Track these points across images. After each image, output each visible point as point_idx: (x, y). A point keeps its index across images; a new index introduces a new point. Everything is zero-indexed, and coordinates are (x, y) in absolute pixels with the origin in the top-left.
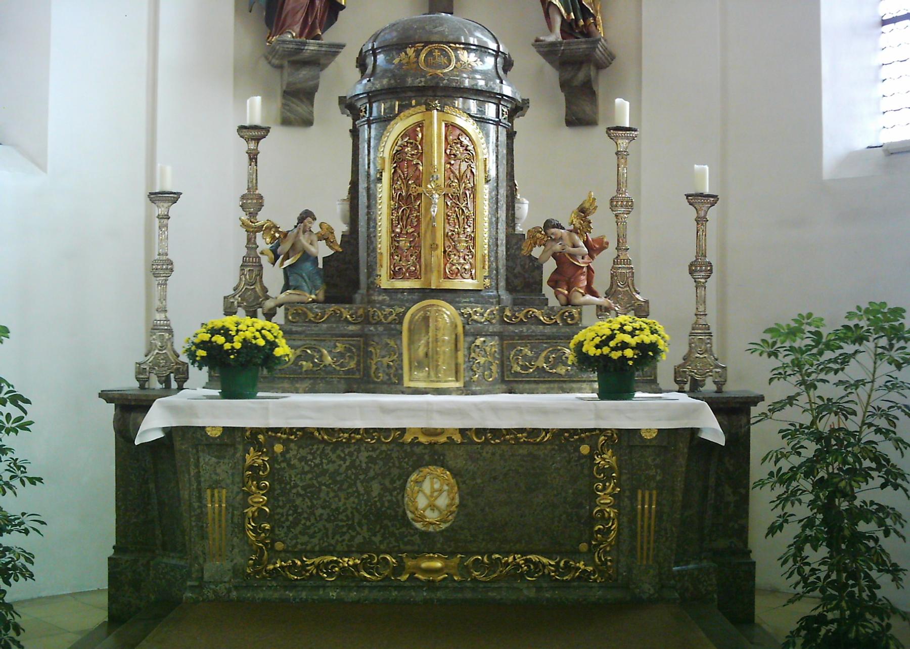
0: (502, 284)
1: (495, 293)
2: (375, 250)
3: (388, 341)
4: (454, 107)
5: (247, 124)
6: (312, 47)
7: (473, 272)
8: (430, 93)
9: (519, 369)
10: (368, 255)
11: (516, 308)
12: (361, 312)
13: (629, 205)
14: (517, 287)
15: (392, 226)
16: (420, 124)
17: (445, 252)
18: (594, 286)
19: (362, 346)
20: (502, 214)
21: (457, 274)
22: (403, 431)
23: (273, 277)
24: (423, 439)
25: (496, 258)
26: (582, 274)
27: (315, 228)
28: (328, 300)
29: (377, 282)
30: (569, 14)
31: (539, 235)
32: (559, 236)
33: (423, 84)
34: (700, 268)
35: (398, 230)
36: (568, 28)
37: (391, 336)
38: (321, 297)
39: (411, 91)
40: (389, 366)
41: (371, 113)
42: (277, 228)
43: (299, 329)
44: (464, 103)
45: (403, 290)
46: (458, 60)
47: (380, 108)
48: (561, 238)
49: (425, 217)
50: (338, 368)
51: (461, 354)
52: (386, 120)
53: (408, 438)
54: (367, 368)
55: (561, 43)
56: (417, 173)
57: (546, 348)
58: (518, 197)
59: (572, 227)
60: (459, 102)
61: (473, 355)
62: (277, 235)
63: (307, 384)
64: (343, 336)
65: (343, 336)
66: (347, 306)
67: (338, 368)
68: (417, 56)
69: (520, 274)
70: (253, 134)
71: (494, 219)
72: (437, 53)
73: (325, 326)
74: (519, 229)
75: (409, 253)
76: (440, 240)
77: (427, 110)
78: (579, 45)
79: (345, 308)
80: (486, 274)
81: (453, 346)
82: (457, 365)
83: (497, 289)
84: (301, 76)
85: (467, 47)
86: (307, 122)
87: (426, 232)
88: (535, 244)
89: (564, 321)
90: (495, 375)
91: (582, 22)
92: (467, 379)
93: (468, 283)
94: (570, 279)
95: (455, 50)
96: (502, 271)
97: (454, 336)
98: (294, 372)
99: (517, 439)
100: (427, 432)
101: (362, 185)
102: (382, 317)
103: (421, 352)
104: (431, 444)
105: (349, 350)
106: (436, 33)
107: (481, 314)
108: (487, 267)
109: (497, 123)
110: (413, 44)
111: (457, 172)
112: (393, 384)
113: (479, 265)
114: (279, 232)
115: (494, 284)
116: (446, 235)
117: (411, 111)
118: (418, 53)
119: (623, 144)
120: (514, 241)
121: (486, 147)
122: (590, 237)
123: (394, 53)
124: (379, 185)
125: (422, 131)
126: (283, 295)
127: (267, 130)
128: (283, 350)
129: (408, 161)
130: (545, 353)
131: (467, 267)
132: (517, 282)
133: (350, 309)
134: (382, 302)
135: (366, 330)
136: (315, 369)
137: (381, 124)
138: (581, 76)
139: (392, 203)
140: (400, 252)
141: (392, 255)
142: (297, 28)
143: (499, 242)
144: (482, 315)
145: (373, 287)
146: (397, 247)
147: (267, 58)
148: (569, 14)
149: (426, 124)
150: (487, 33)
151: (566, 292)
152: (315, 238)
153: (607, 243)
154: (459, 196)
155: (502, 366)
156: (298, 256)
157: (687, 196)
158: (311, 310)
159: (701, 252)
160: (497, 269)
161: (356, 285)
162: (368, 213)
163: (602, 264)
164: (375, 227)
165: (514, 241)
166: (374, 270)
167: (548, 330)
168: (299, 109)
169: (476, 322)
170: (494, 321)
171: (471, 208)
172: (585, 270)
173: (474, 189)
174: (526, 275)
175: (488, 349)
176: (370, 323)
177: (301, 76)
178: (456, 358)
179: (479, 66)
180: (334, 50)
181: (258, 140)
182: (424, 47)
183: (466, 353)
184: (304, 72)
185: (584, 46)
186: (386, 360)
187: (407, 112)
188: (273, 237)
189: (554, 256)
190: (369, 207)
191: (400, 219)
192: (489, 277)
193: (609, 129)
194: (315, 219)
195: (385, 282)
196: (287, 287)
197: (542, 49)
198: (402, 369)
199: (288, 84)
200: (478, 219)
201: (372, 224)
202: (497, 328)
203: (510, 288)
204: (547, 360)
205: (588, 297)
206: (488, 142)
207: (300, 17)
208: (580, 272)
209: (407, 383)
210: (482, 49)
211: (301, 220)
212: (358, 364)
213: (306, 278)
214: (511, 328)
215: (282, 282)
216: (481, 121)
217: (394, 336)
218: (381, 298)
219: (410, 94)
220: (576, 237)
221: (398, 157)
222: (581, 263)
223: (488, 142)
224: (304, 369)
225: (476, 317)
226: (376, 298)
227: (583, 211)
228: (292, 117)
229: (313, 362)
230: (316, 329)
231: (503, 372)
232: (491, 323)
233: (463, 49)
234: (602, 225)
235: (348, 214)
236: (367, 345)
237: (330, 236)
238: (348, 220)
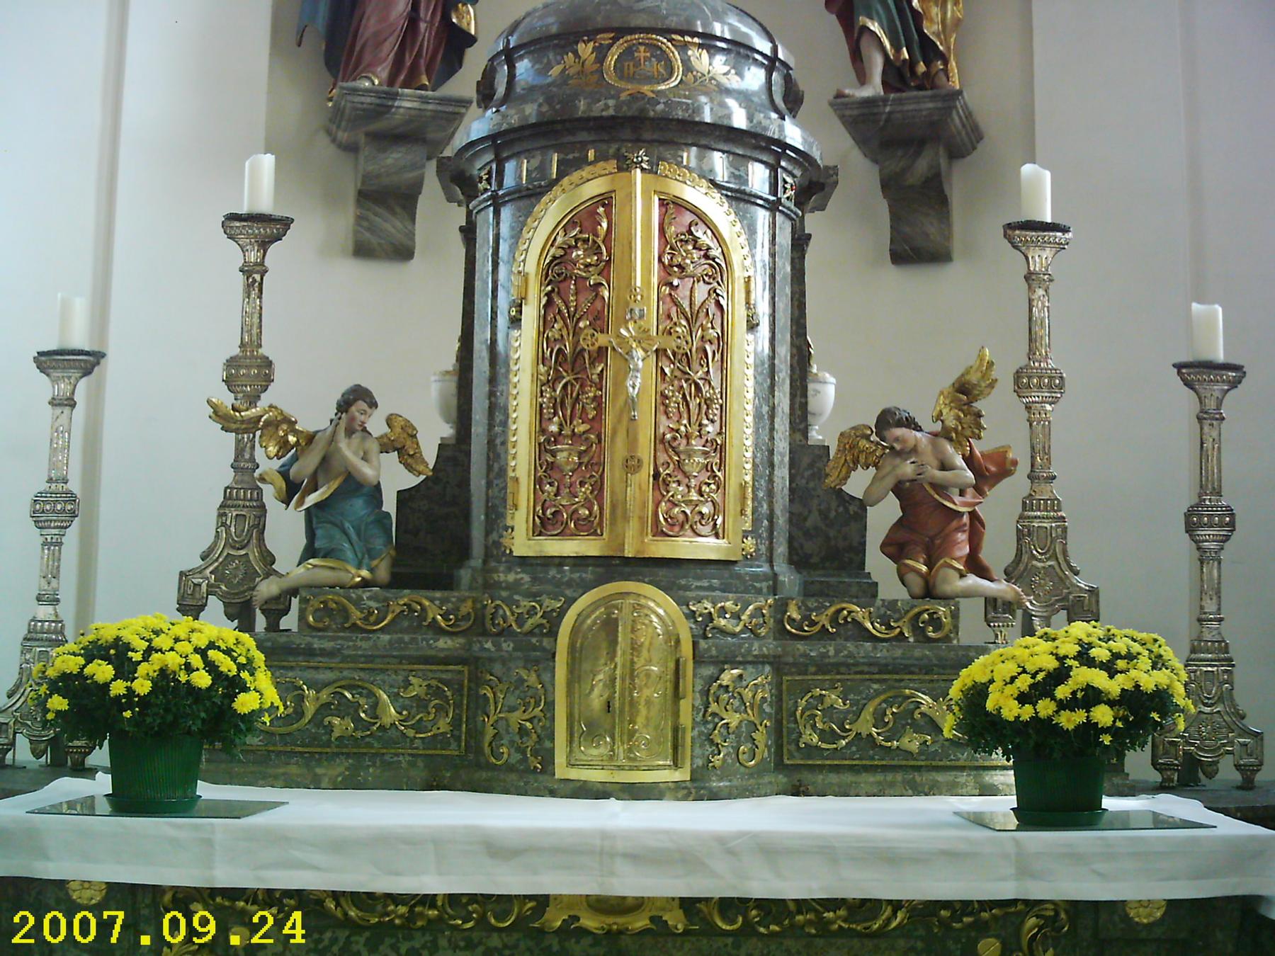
0: (781, 549)
1: (765, 568)
2: (503, 472)
3: (524, 674)
4: (679, 164)
5: (244, 210)
6: (407, 102)
7: (719, 521)
8: (627, 133)
9: (815, 738)
10: (489, 484)
11: (812, 603)
12: (466, 608)
13: (1056, 384)
14: (811, 556)
15: (541, 417)
16: (605, 200)
17: (656, 475)
18: (985, 556)
19: (466, 682)
20: (783, 399)
21: (683, 525)
22: (542, 902)
23: (285, 529)
24: (590, 922)
25: (770, 493)
26: (960, 529)
27: (377, 425)
28: (398, 581)
29: (505, 541)
30: (898, 50)
31: (863, 443)
32: (911, 444)
33: (611, 112)
34: (1208, 520)
35: (554, 428)
36: (897, 76)
37: (530, 663)
38: (383, 573)
39: (589, 130)
40: (522, 731)
41: (500, 185)
42: (292, 423)
43: (328, 645)
44: (700, 158)
45: (561, 561)
46: (687, 64)
47: (515, 172)
48: (914, 450)
49: (616, 395)
50: (411, 733)
51: (685, 706)
52: (530, 195)
53: (555, 919)
54: (475, 734)
55: (885, 101)
56: (598, 305)
57: (878, 693)
58: (814, 370)
59: (938, 427)
60: (690, 156)
61: (714, 707)
62: (292, 439)
63: (339, 768)
64: (427, 660)
65: (427, 660)
66: (438, 594)
67: (411, 733)
68: (601, 59)
69: (818, 531)
71: (765, 409)
72: (642, 53)
73: (386, 638)
74: (816, 435)
75: (577, 479)
76: (645, 450)
77: (620, 169)
78: (919, 104)
79: (432, 600)
80: (748, 526)
81: (670, 686)
82: (676, 730)
83: (771, 561)
84: (389, 161)
85: (709, 42)
86: (404, 253)
87: (614, 432)
88: (856, 462)
89: (919, 631)
90: (762, 752)
91: (921, 68)
92: (700, 762)
93: (705, 546)
94: (932, 539)
95: (683, 47)
96: (781, 521)
97: (672, 665)
98: (314, 739)
99: (823, 925)
100: (601, 905)
101: (482, 335)
102: (511, 620)
103: (596, 700)
104: (612, 936)
105: (438, 693)
106: (639, 11)
107: (735, 615)
108: (749, 511)
109: (773, 207)
110: (592, 34)
111: (686, 305)
112: (530, 774)
113: (732, 506)
114: (296, 432)
115: (763, 548)
116: (660, 440)
117: (585, 172)
118: (601, 53)
119: (1041, 258)
120: (806, 461)
122: (979, 448)
123: (551, 56)
124: (515, 333)
125: (608, 215)
126: (301, 570)
127: (286, 223)
128: (261, 694)
129: (578, 281)
130: (877, 701)
131: (705, 510)
132: (810, 547)
133: (444, 601)
134: (514, 587)
135: (476, 647)
136: (359, 734)
137: (526, 202)
138: (922, 166)
139: (542, 369)
140: (556, 475)
141: (538, 482)
142: (383, 71)
143: (776, 459)
144: (736, 616)
145: (496, 552)
146: (552, 466)
147: (329, 132)
148: (898, 50)
149: (618, 199)
150: (750, 21)
151: (924, 568)
152: (374, 447)
153: (1015, 463)
154: (690, 360)
155: (778, 732)
156: (334, 485)
157: (1179, 367)
158: (357, 603)
159: (1209, 485)
160: (771, 517)
161: (462, 550)
162: (492, 394)
163: (1000, 509)
164: (505, 424)
166: (502, 516)
167: (882, 653)
168: (388, 226)
169: (723, 632)
170: (763, 631)
171: (716, 382)
172: (966, 519)
173: (722, 341)
174: (832, 533)
175: (748, 694)
176: (485, 633)
177: (389, 161)
178: (676, 714)
179: (734, 82)
180: (450, 109)
181: (264, 245)
182: (615, 39)
183: (698, 703)
184: (395, 155)
185: (931, 105)
186: (516, 718)
187: (576, 176)
188: (284, 446)
189: (898, 489)
190: (493, 380)
191: (558, 404)
192: (754, 532)
193: (1010, 226)
194: (373, 405)
195: (522, 543)
196: (310, 552)
197: (848, 113)
198: (552, 737)
199: (366, 177)
200: (733, 406)
201: (499, 417)
202: (770, 646)
203: (798, 560)
204: (879, 720)
205: (972, 580)
206: (752, 244)
207: (389, 49)
208: (955, 524)
209: (562, 770)
210: (740, 50)
211: (344, 406)
212: (456, 723)
213: (352, 531)
214: (801, 647)
215: (302, 541)
216: (739, 197)
217: (537, 662)
218: (511, 577)
219: (583, 136)
220: (949, 448)
221: (557, 272)
222: (958, 504)
223: (752, 244)
224: (336, 734)
225: (723, 622)
226: (502, 577)
227: (965, 392)
228: (374, 240)
229: (357, 720)
230: (364, 645)
231: (779, 747)
232: (757, 636)
233: (700, 46)
235: (454, 402)
236: (476, 680)
237: (409, 443)
238: (454, 413)
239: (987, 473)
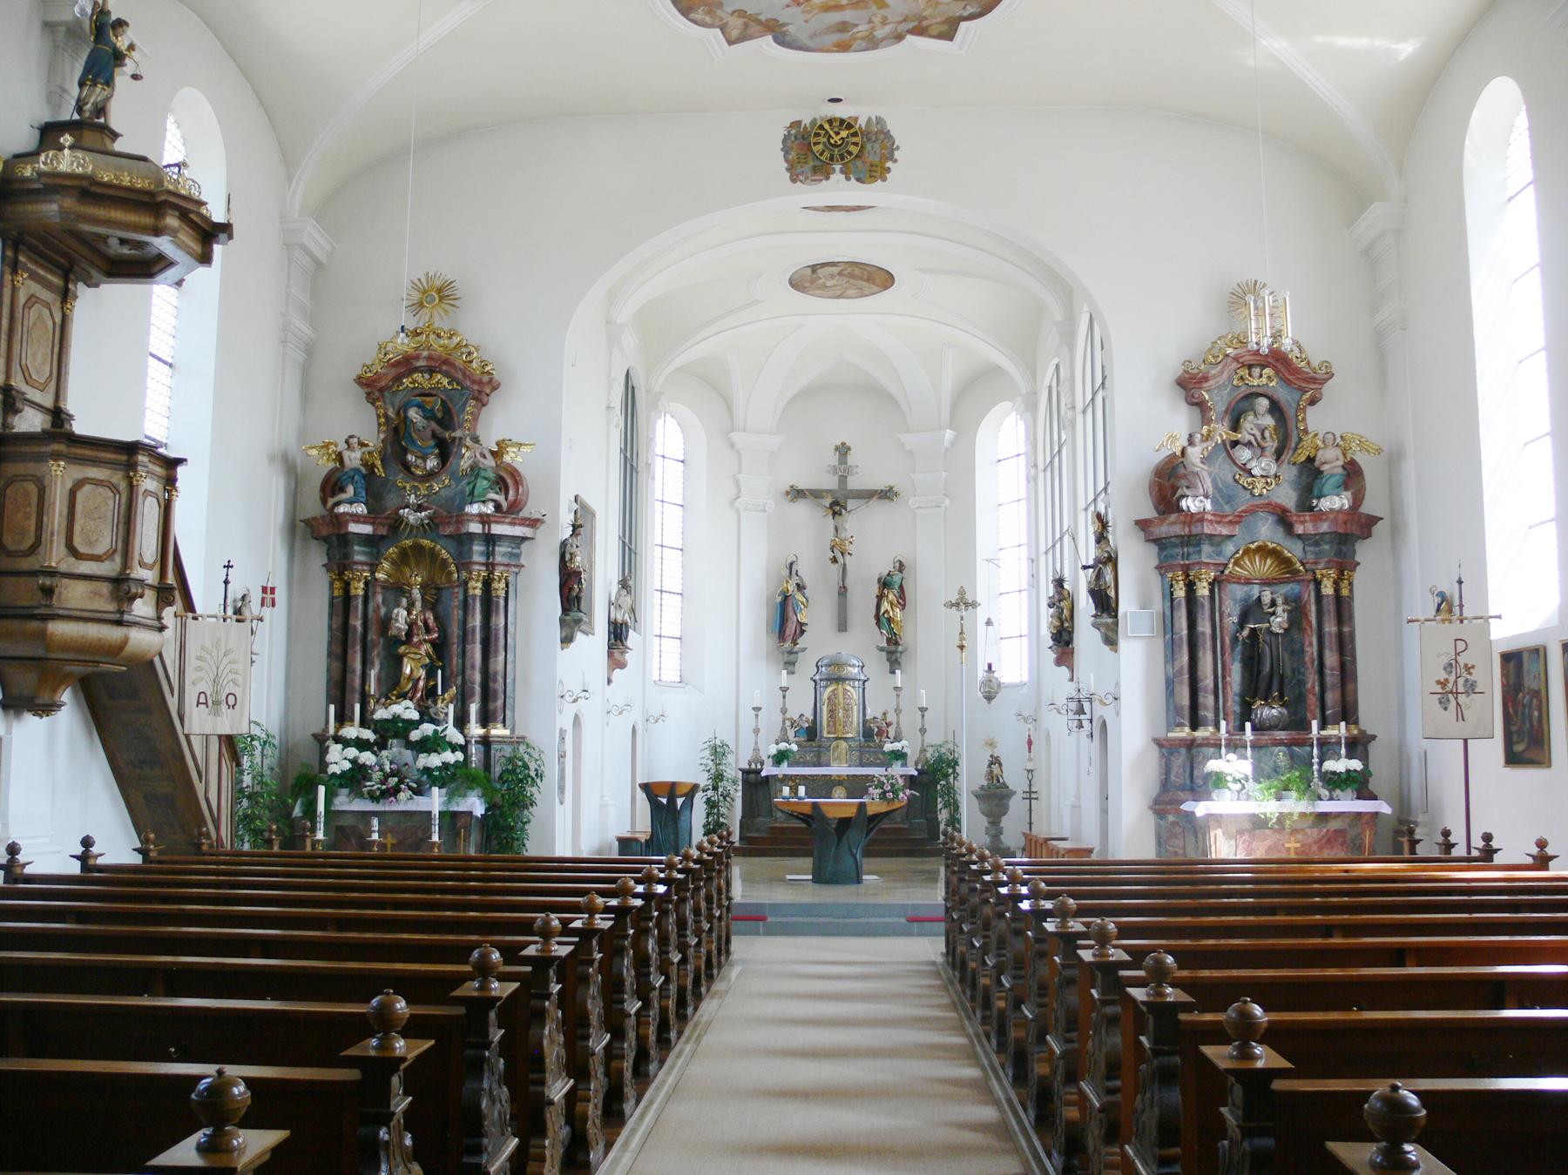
23: (791, 733)
36: (889, 641)
69: (868, 733)
70: (784, 690)
78: (892, 648)
112: (828, 765)
121: (854, 693)
154: (847, 710)
165: (865, 721)
234: (891, 717)
239: (888, 725)
